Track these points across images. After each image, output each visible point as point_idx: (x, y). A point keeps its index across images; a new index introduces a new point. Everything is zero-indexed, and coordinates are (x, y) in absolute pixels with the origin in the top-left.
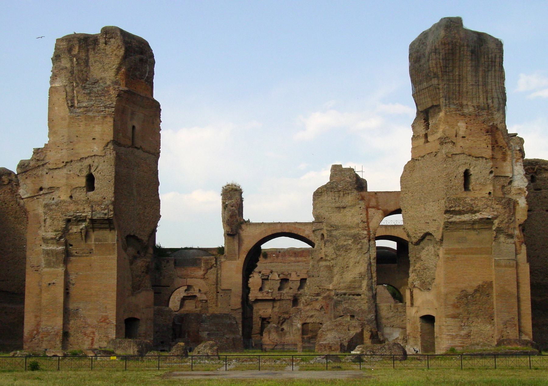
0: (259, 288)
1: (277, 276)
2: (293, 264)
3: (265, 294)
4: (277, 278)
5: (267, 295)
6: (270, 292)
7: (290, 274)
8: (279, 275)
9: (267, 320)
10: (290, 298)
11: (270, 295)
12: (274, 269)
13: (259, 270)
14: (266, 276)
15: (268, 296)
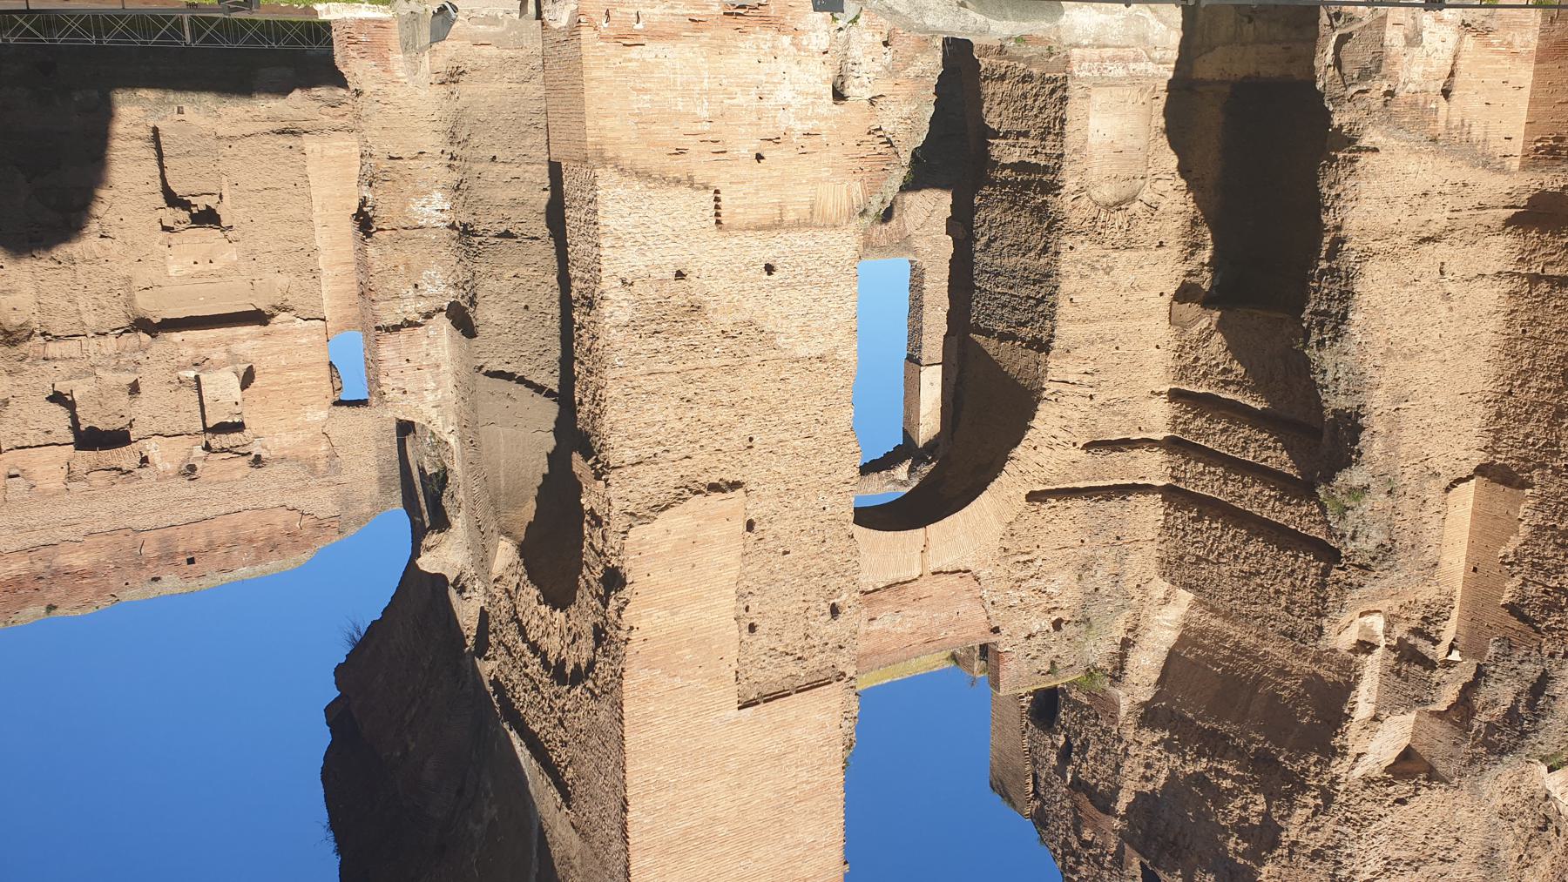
0: (257, 382)
1: (154, 456)
2: (68, 533)
3: (218, 355)
4: (153, 448)
5: (204, 352)
6: (185, 368)
7: (70, 476)
8: (145, 460)
9: (183, 215)
10: (53, 349)
11: (188, 353)
12: (184, 488)
13: (264, 470)
14: (222, 450)
15: (198, 346)
